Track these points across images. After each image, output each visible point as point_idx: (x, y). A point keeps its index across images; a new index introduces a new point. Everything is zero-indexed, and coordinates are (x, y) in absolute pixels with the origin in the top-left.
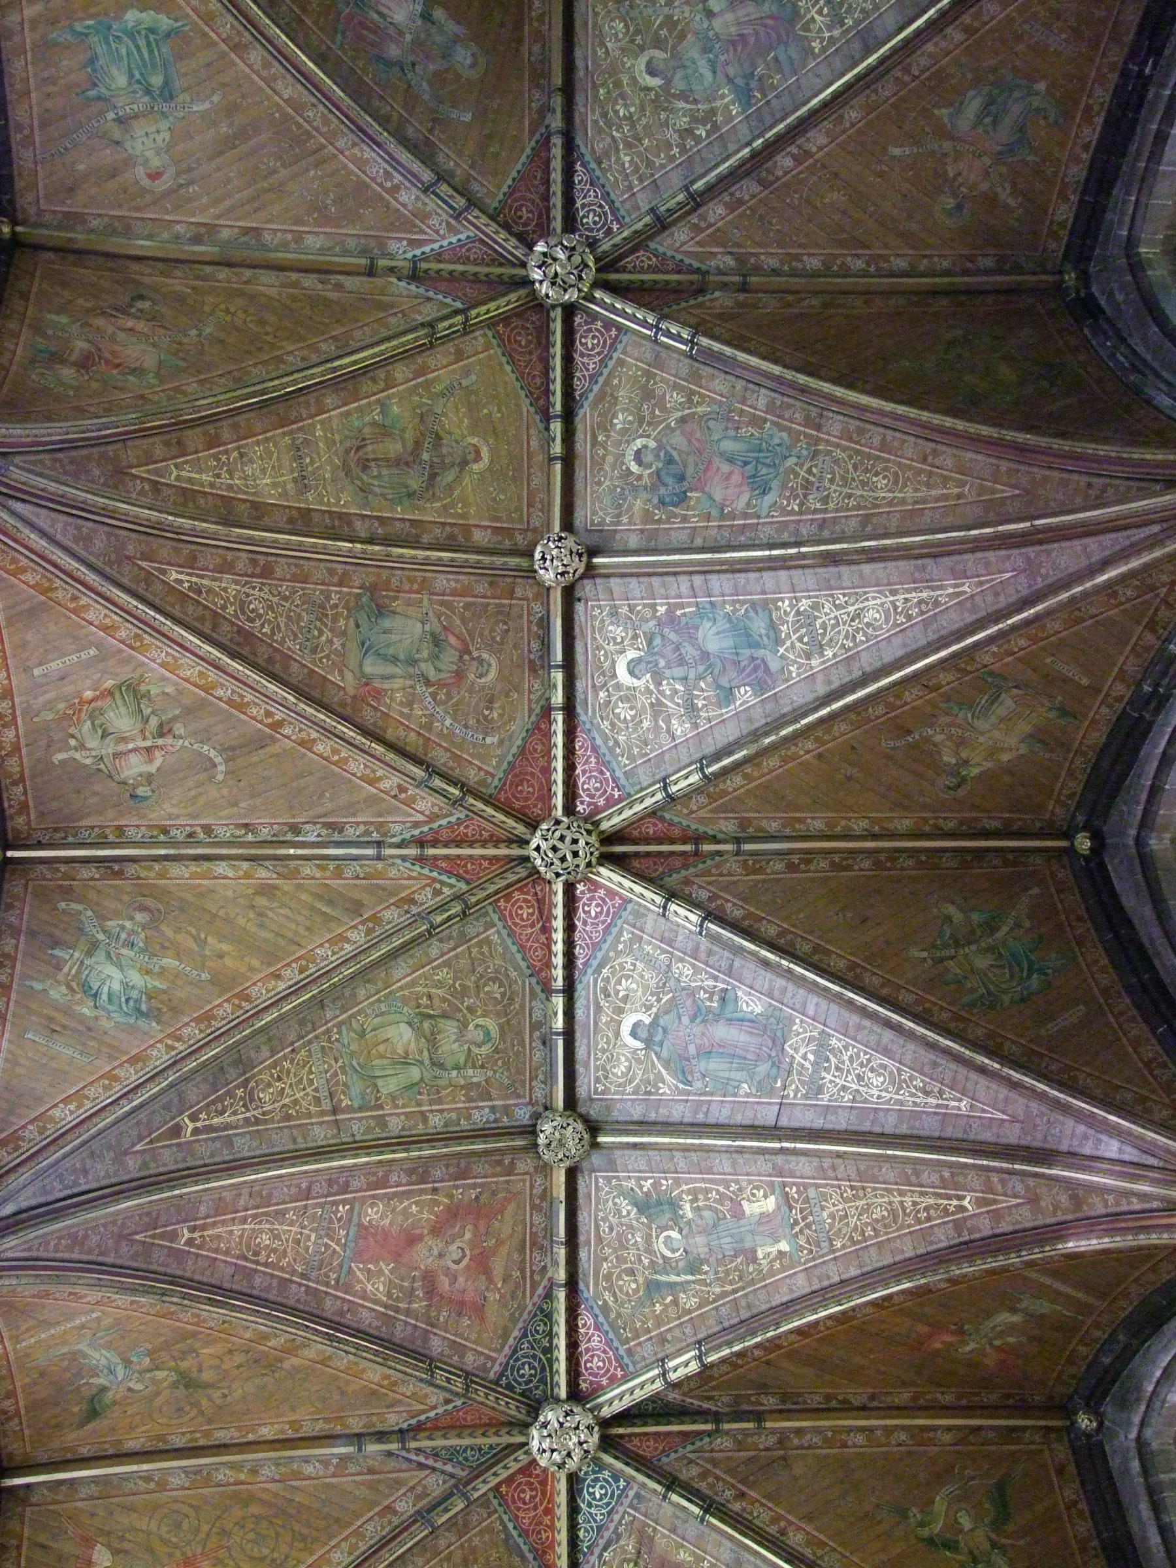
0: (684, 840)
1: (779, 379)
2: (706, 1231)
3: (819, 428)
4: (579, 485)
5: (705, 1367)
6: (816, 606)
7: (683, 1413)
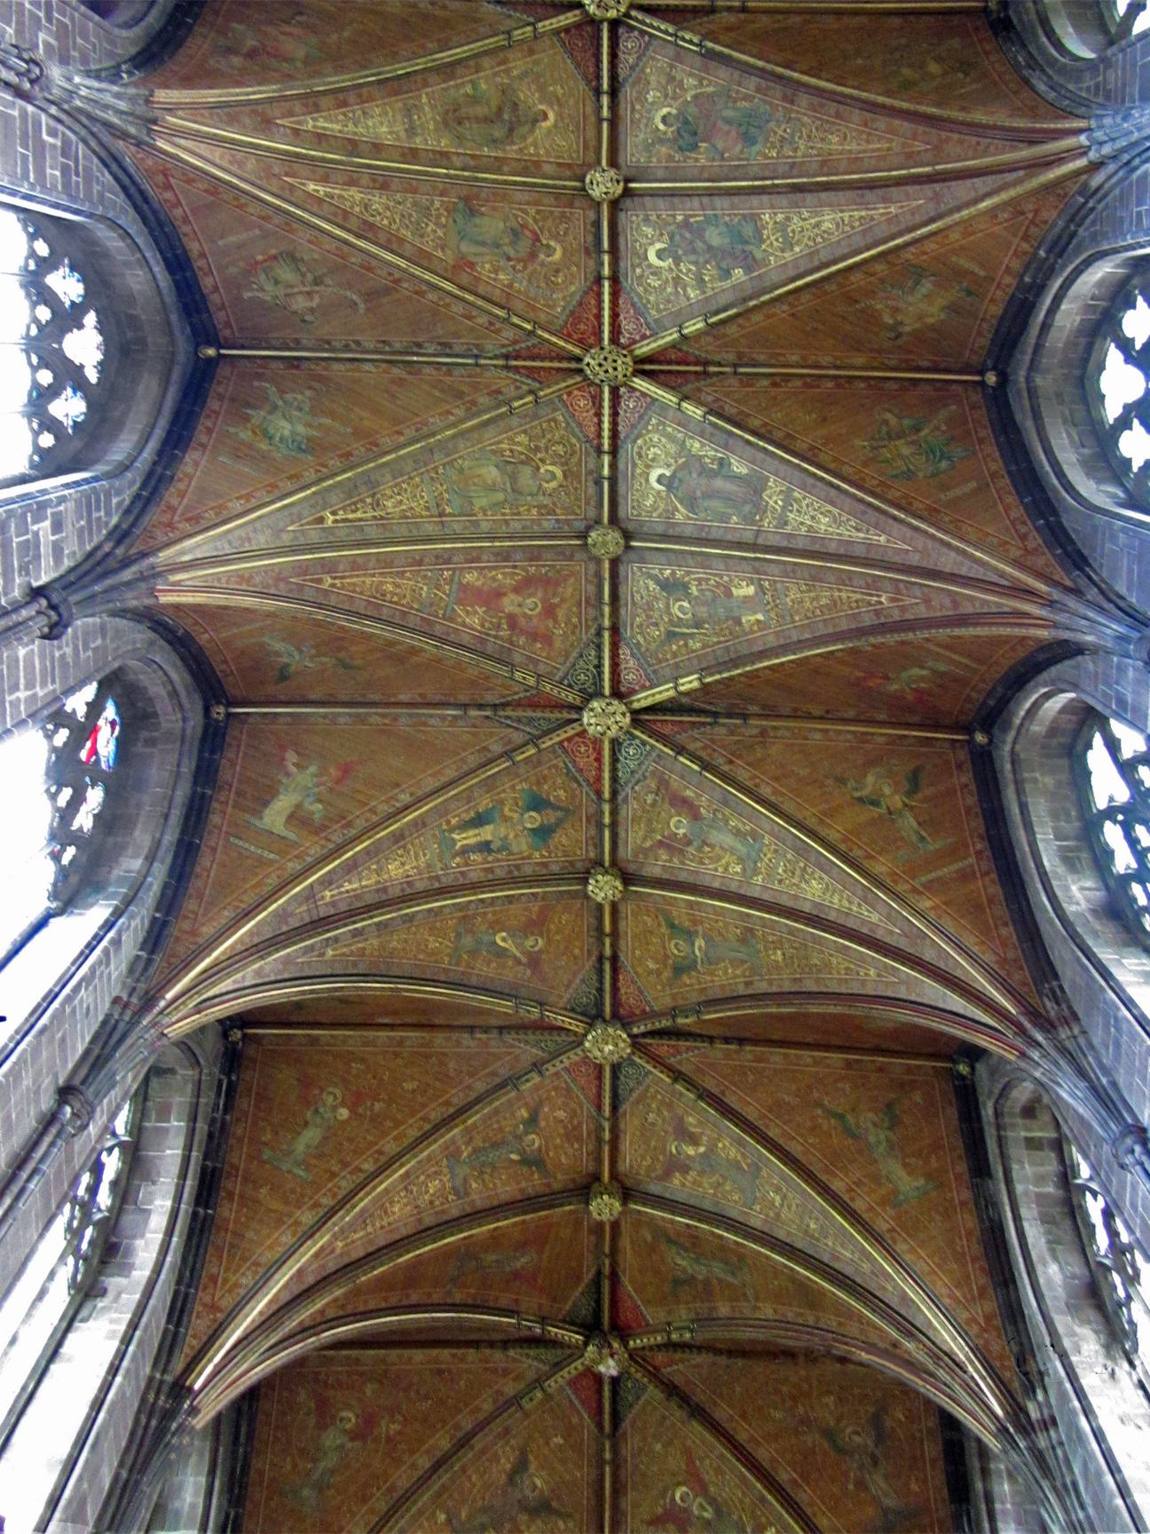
0: (697, 363)
1: (763, 70)
2: (706, 603)
3: (792, 102)
4: (622, 137)
5: (705, 686)
6: (788, 219)
7: (691, 710)
